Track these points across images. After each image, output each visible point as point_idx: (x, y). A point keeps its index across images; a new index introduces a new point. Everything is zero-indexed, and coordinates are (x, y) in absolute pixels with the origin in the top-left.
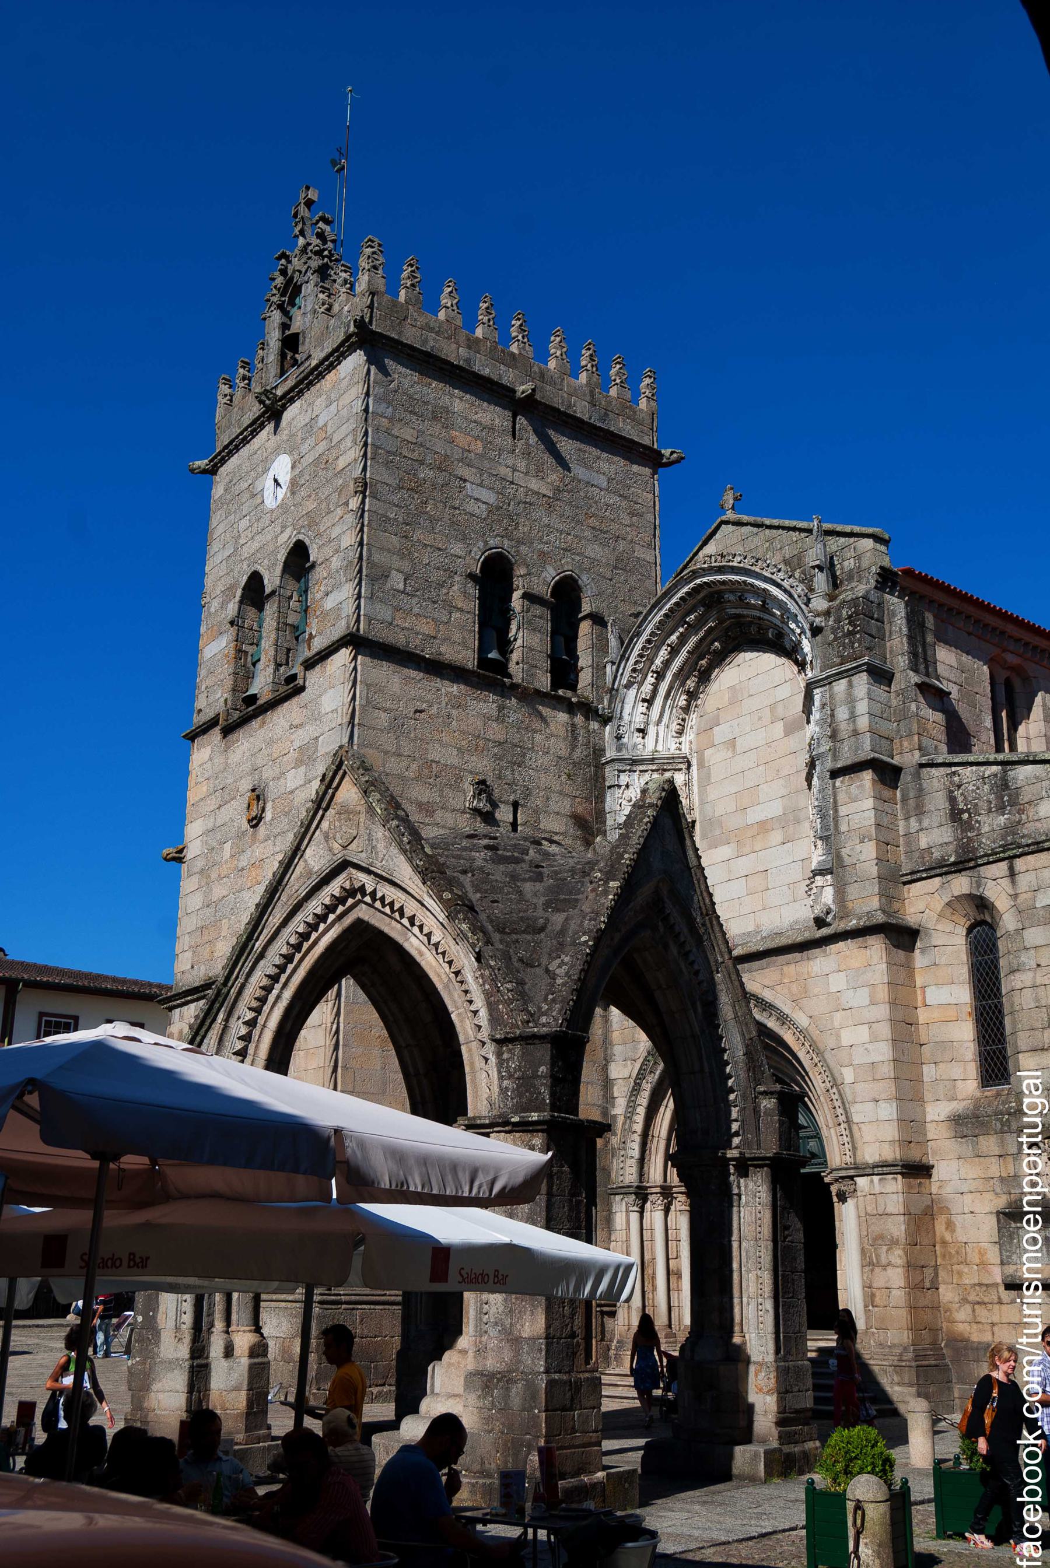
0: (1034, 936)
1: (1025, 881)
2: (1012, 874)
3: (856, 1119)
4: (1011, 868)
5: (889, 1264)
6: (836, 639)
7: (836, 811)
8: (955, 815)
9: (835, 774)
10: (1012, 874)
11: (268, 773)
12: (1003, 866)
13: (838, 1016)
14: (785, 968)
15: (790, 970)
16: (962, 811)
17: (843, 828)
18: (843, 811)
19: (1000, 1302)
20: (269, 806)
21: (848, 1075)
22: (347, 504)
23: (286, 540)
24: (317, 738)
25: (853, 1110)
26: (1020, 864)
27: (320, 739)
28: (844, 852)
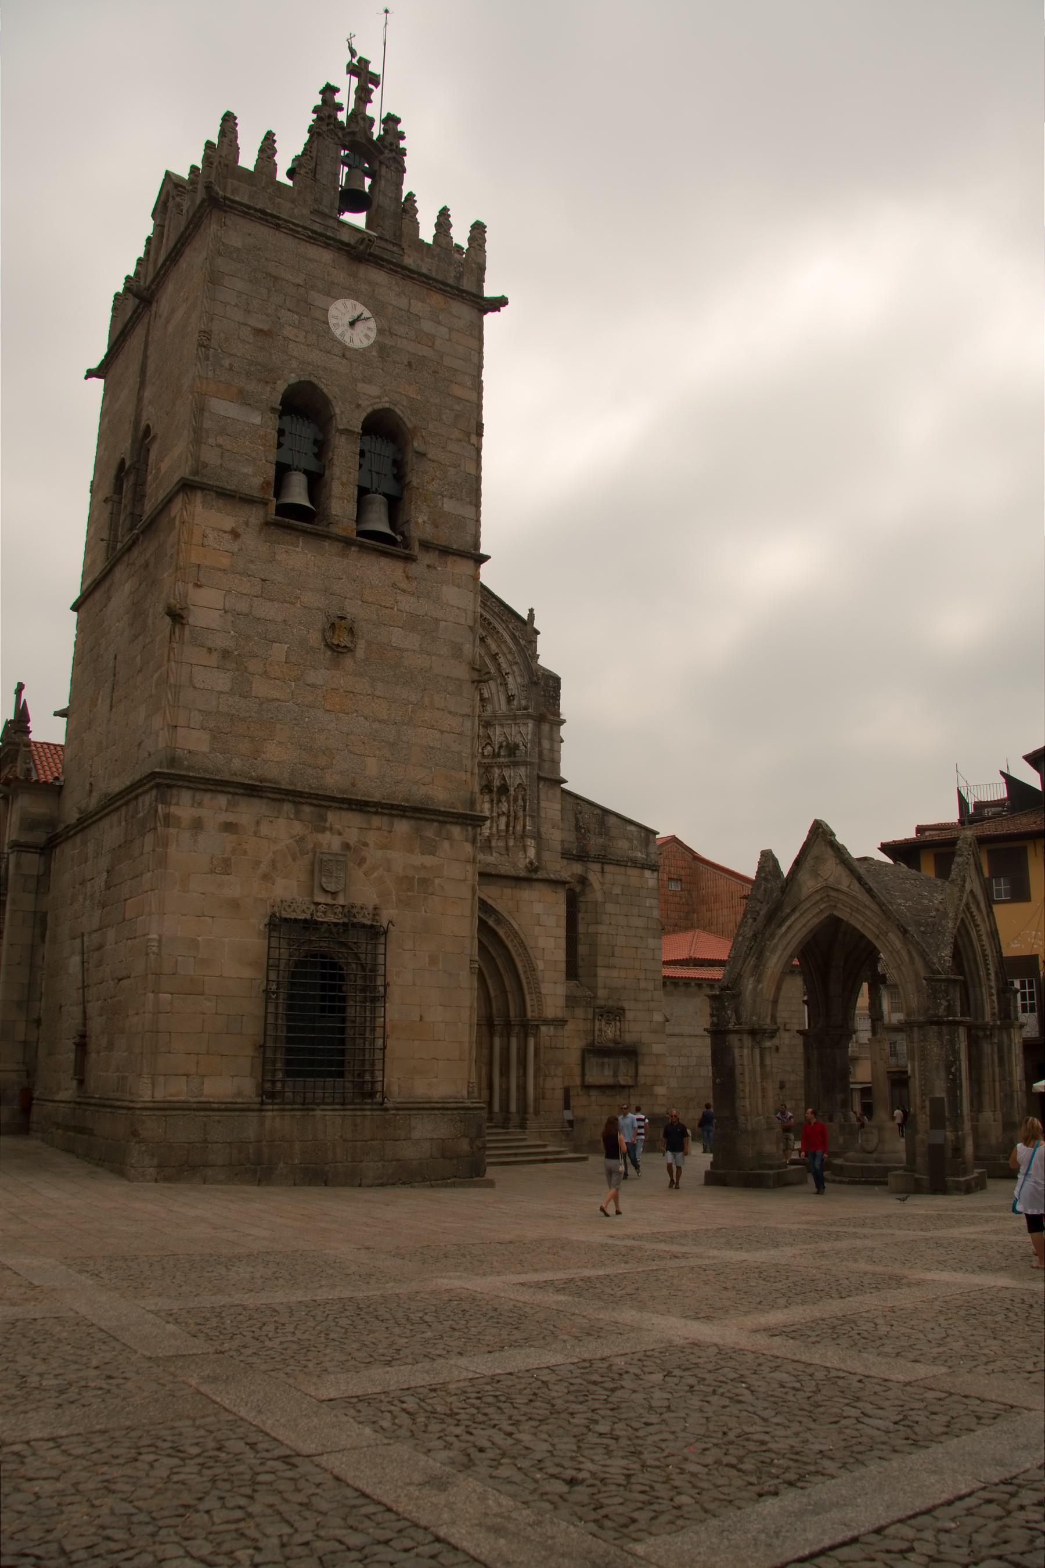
0: (610, 908)
1: (608, 877)
2: (603, 872)
3: (543, 991)
4: (603, 869)
5: (556, 1075)
6: (544, 696)
7: (539, 803)
8: (578, 828)
9: (540, 778)
10: (603, 872)
11: (353, 609)
12: (599, 865)
13: (537, 928)
14: (505, 890)
15: (508, 891)
16: (581, 828)
17: (543, 815)
18: (543, 804)
19: (578, 1095)
20: (361, 645)
21: (540, 965)
22: (469, 435)
23: (373, 395)
24: (437, 620)
25: (542, 986)
26: (607, 868)
27: (442, 624)
28: (543, 830)
